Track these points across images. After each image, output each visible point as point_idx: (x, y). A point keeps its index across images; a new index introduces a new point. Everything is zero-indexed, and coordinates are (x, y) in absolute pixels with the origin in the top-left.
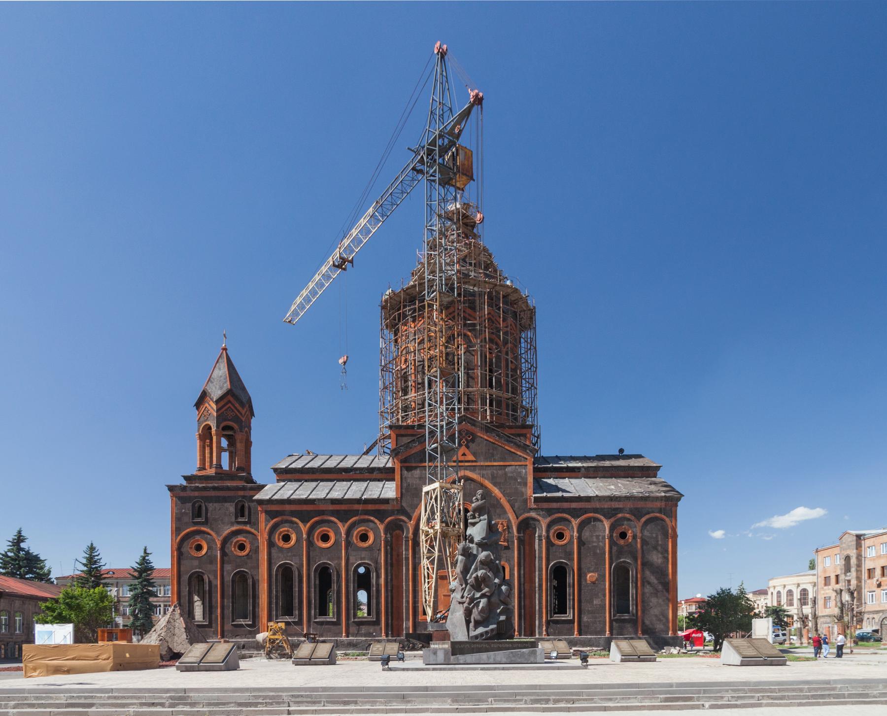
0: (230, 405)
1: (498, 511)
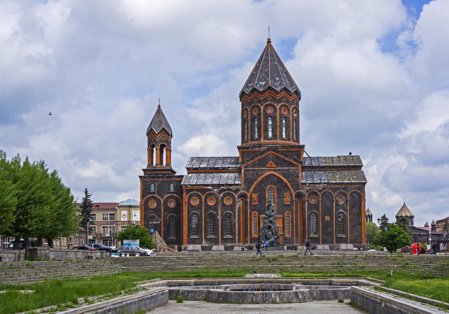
0: (163, 135)
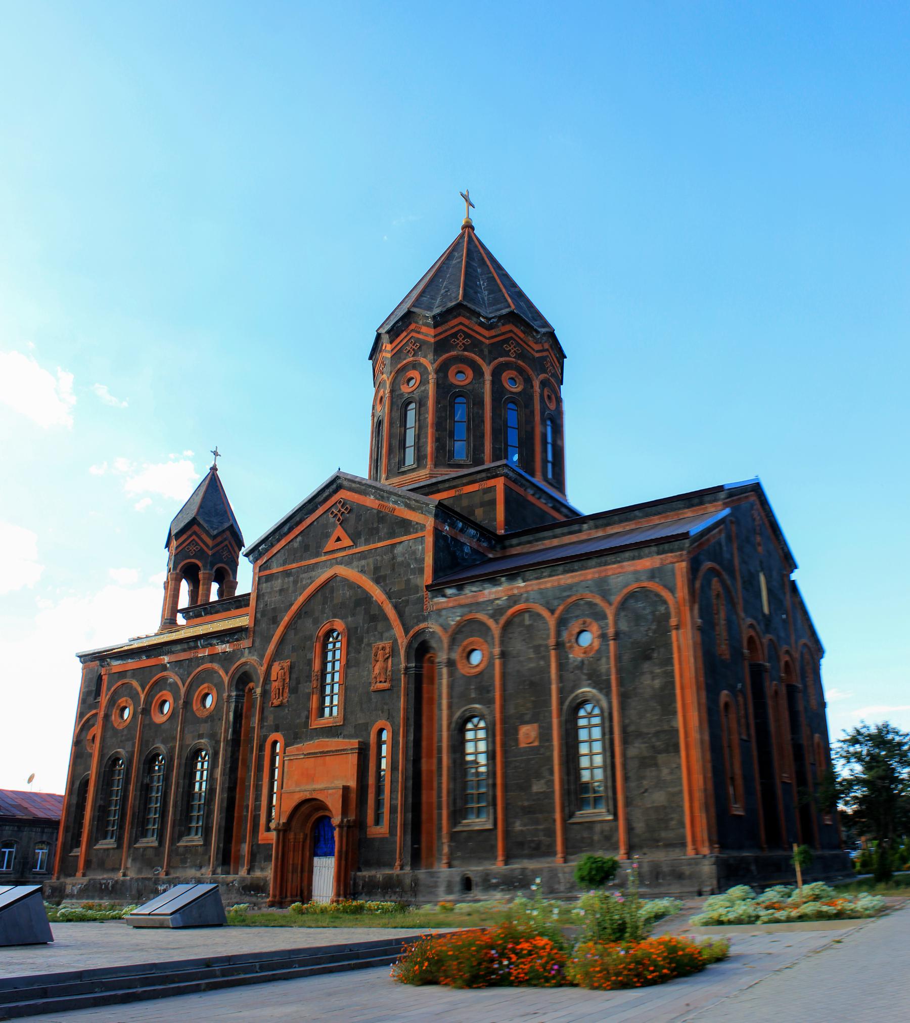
1: (380, 626)
